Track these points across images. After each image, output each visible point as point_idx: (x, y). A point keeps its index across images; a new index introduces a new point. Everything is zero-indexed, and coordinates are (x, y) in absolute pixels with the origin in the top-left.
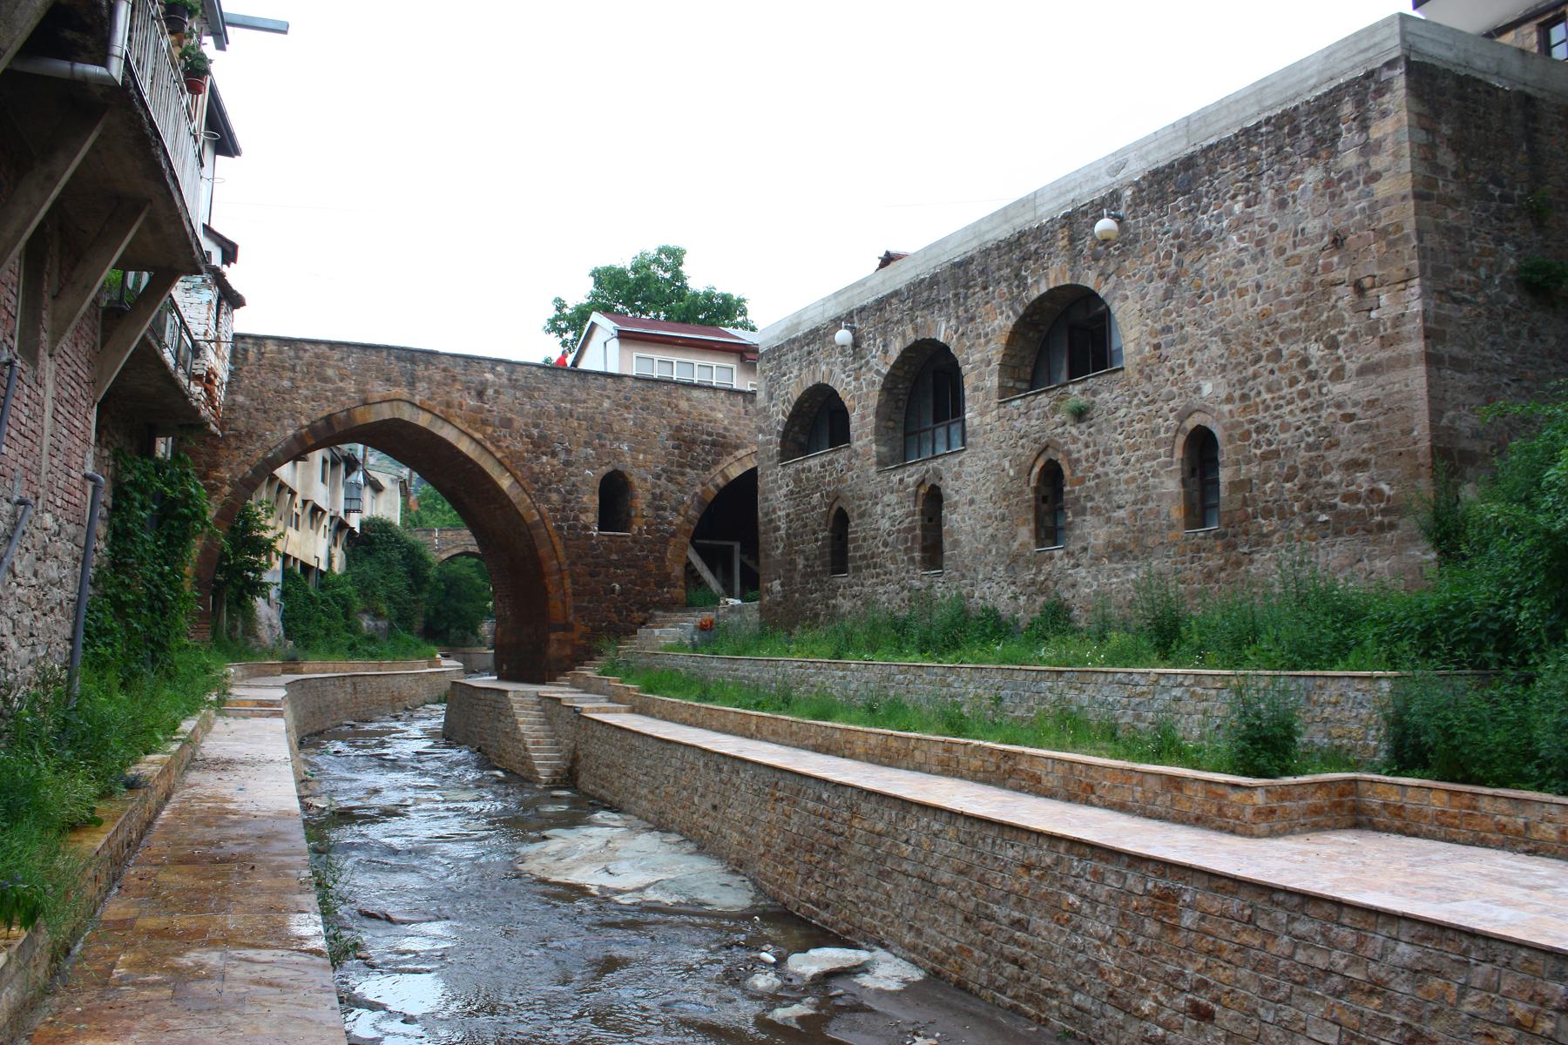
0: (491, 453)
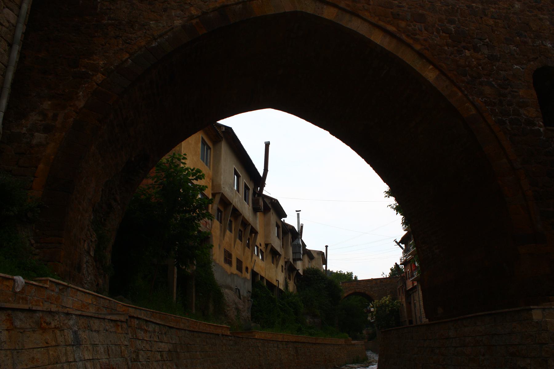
0: (409, 46)
